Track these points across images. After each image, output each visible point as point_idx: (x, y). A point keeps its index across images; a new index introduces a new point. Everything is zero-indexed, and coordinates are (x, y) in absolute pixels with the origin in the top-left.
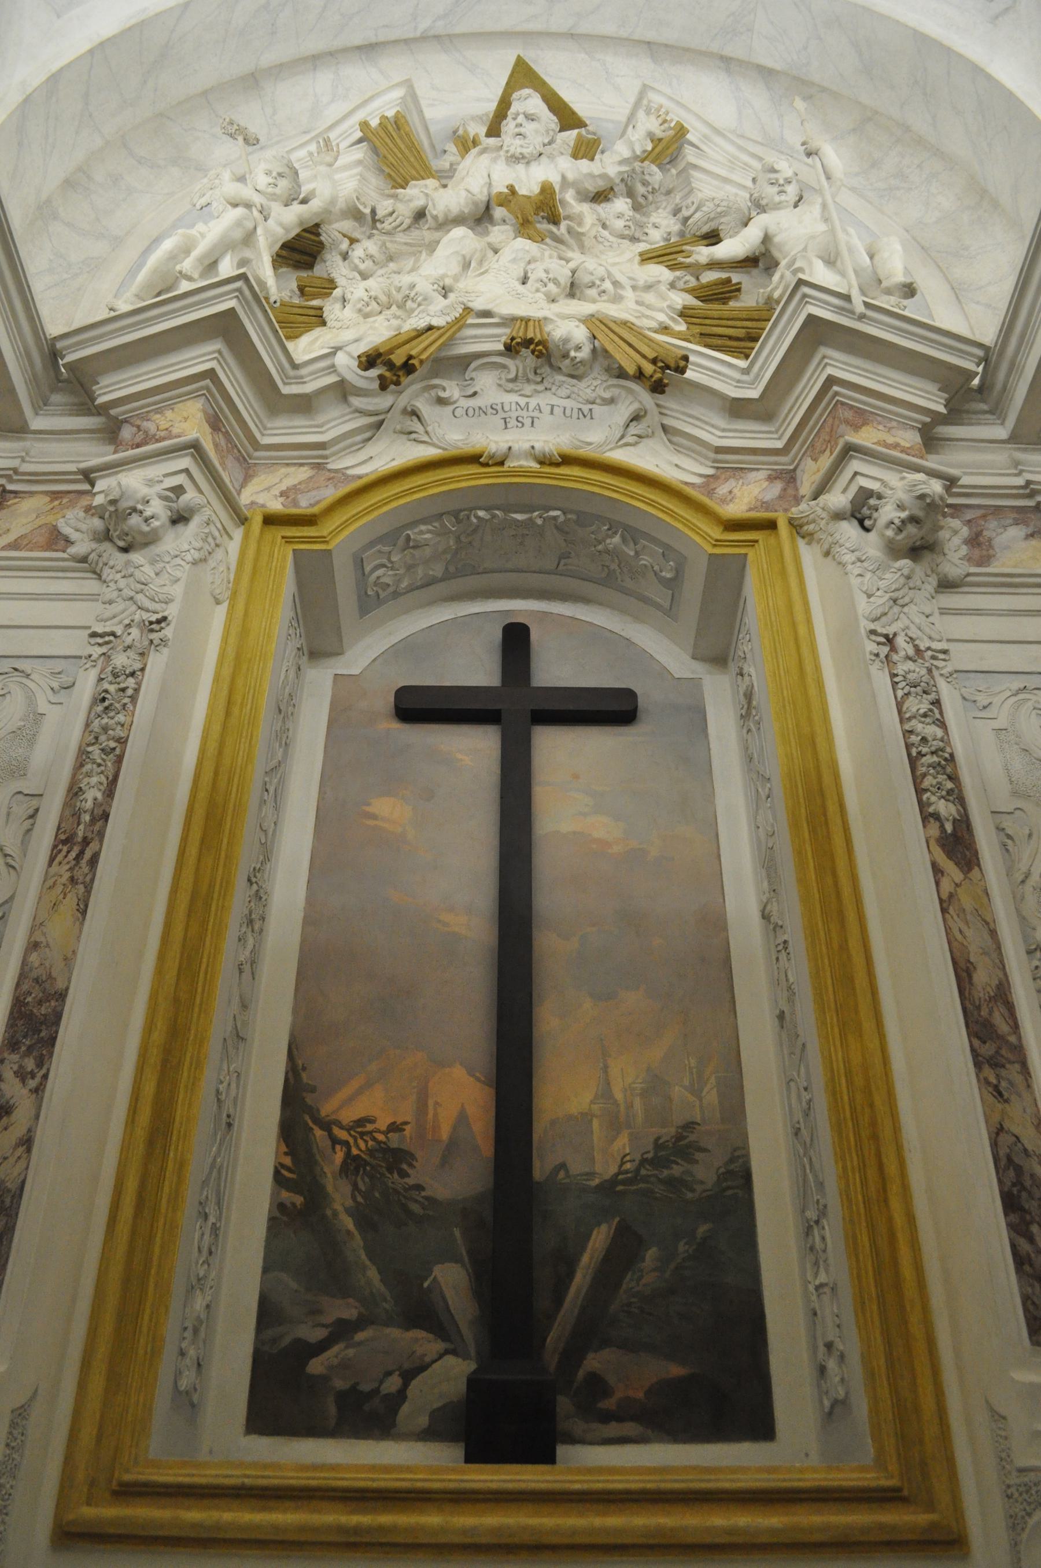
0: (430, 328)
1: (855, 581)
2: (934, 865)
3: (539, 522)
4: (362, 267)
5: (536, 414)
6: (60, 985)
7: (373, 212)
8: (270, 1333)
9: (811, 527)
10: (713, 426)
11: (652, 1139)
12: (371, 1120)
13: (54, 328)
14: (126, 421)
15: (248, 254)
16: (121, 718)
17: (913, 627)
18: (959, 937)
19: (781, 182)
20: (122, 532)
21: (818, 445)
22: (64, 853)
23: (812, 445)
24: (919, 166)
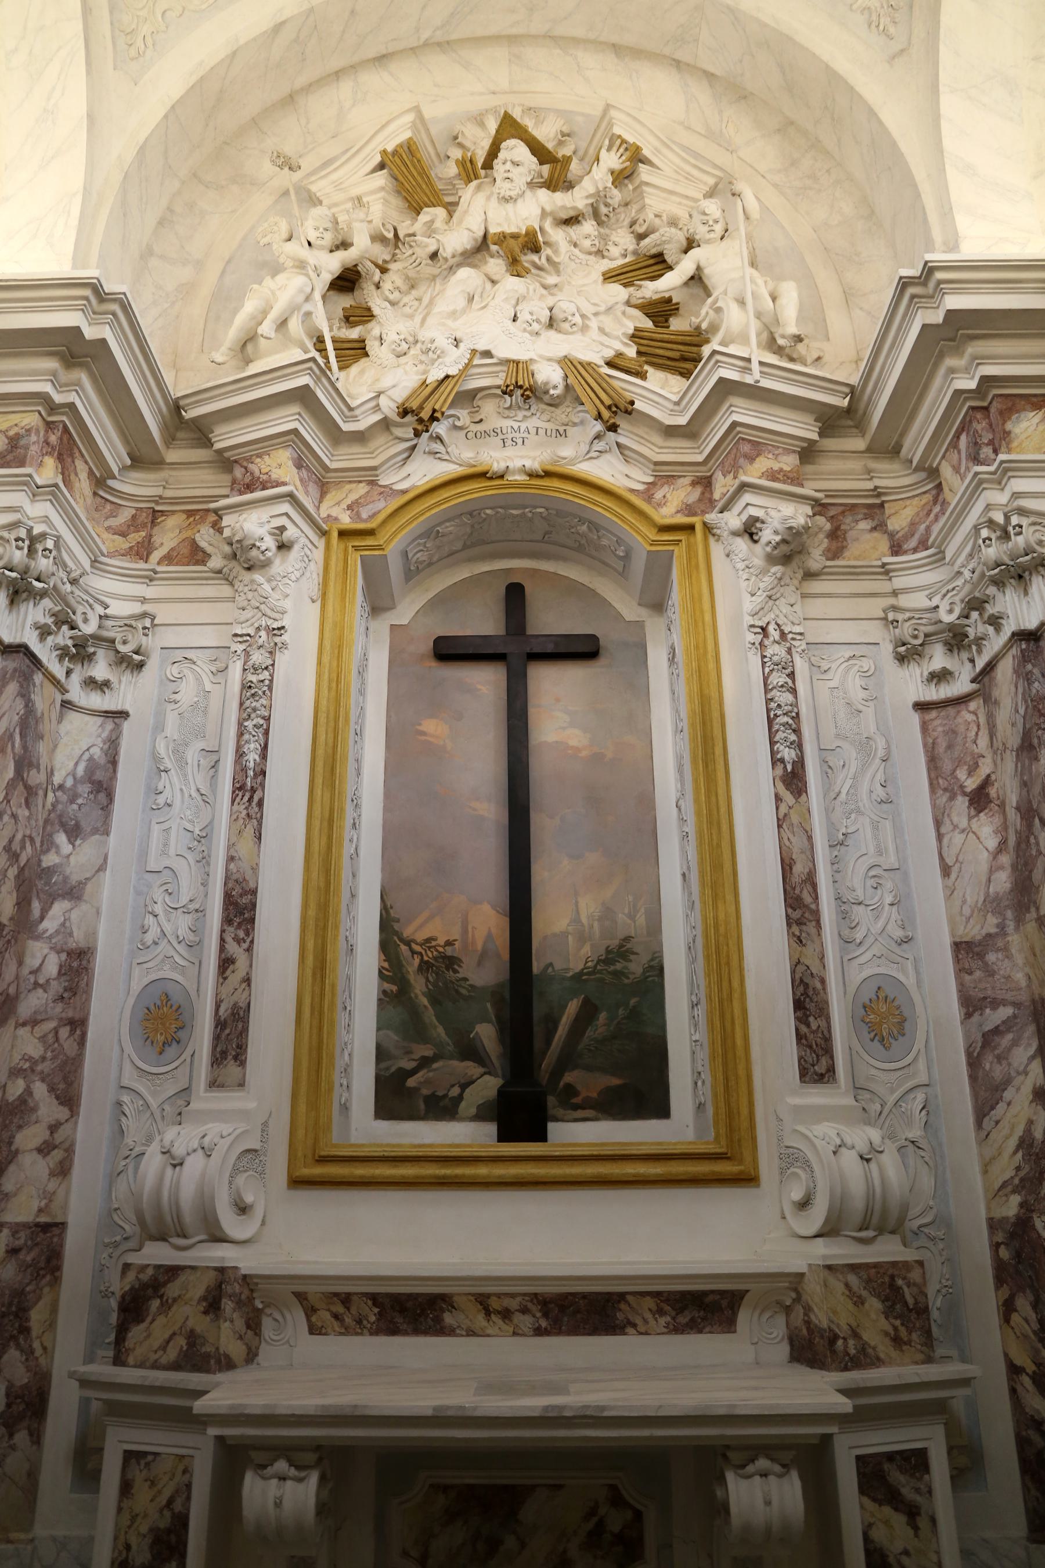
0: (447, 377)
1: (744, 584)
2: (777, 796)
3: (530, 515)
4: (391, 297)
5: (526, 435)
6: (252, 885)
7: (396, 235)
8: (383, 1065)
9: (718, 532)
11: (604, 947)
12: (435, 939)
13: (177, 390)
14: (236, 461)
15: (307, 307)
16: (263, 701)
17: (781, 616)
18: (787, 843)
19: (711, 223)
20: (244, 557)
21: (727, 464)
22: (240, 797)
23: (722, 462)
24: (828, 171)
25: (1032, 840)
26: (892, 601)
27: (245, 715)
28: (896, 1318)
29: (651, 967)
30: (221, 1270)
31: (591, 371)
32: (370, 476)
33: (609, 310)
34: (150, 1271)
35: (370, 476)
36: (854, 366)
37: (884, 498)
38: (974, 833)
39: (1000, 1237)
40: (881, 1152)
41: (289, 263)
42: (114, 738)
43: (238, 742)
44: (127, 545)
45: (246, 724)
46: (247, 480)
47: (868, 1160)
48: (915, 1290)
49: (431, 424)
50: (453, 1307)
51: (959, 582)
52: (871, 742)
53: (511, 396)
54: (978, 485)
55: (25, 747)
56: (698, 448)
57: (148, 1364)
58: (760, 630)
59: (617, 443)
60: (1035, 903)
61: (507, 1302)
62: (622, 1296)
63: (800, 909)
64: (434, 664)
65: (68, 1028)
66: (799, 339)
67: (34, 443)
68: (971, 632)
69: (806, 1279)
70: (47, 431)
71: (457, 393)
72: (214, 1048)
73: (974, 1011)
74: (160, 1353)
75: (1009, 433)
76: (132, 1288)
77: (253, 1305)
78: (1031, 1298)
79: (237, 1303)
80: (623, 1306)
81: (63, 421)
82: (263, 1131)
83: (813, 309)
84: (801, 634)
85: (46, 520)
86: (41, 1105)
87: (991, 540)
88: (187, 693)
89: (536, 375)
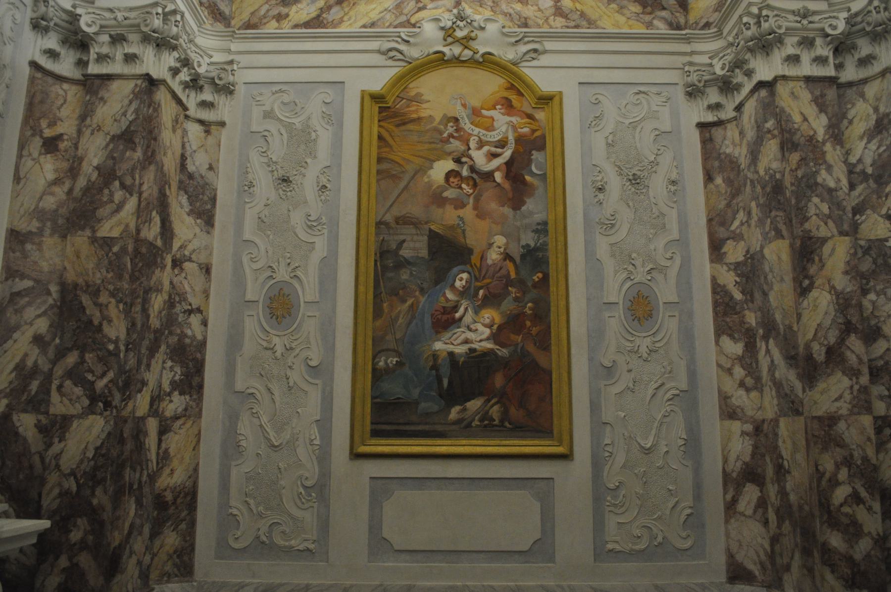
25: (106, 191)
51: (108, 15)
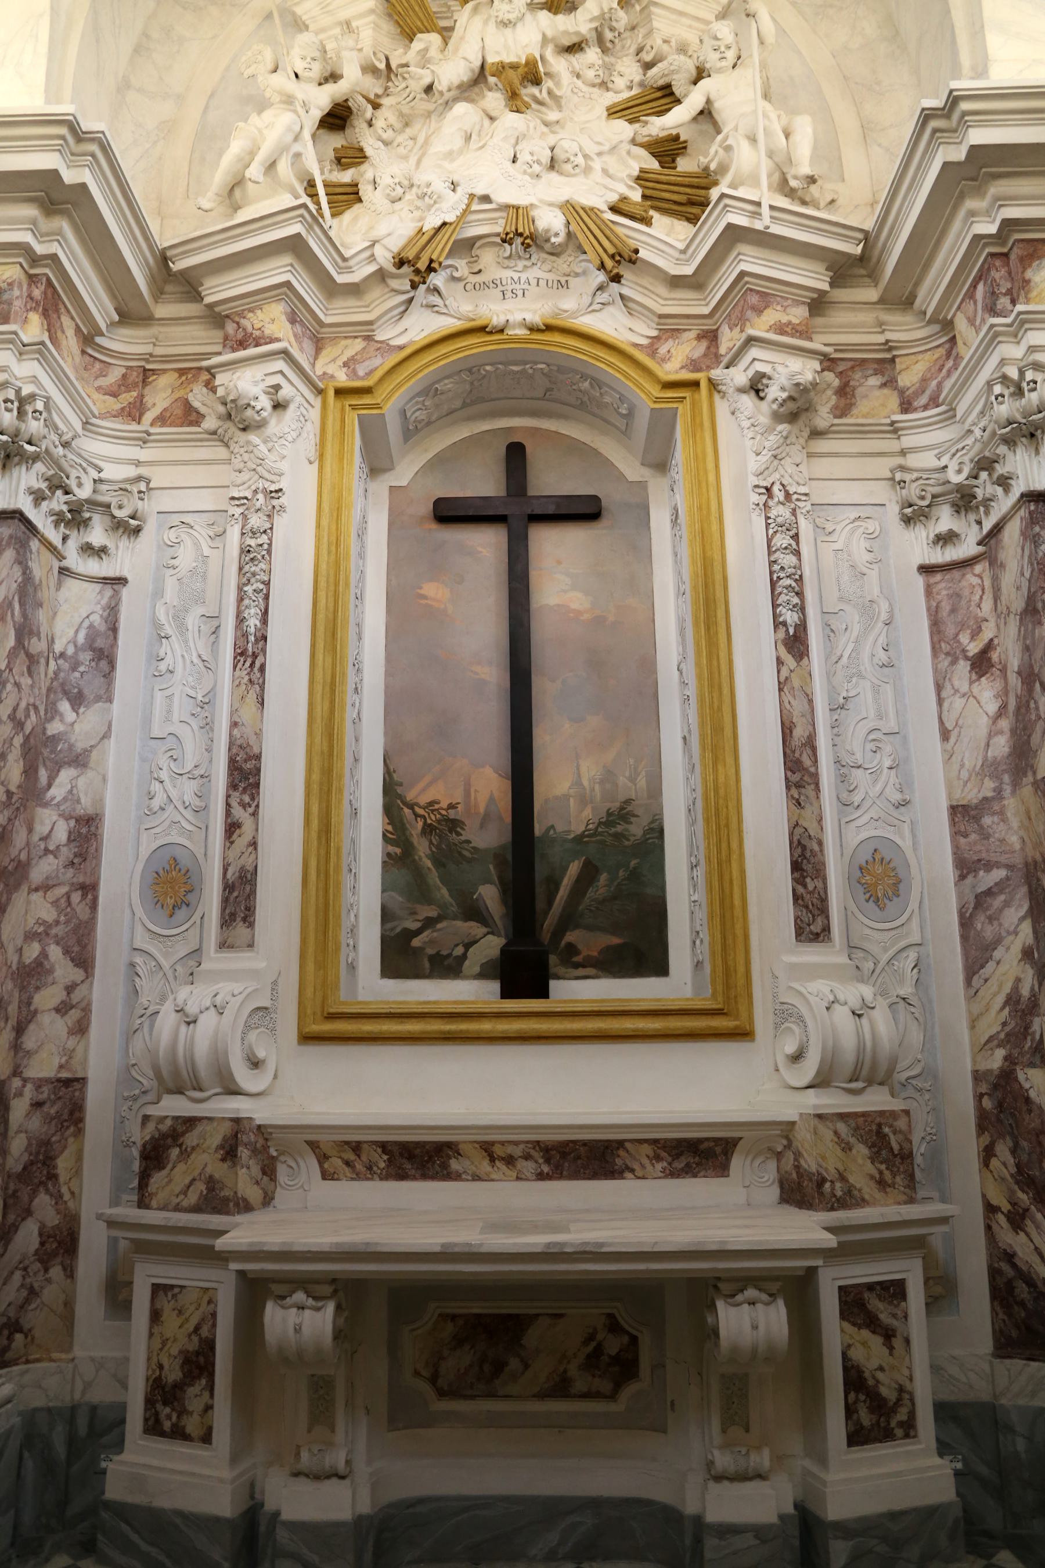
0: (444, 224)
2: (778, 659)
3: (530, 371)
4: (385, 136)
5: (526, 286)
6: (256, 750)
7: (388, 66)
8: (389, 926)
9: (723, 388)
10: (657, 295)
11: (605, 810)
13: (164, 241)
14: (227, 316)
15: (297, 148)
16: (262, 566)
17: (787, 476)
18: (788, 707)
20: (239, 418)
21: (733, 317)
23: (729, 315)
25: (1032, 705)
26: (899, 460)
27: (244, 580)
28: (881, 1163)
29: (652, 829)
30: (237, 1121)
31: (594, 217)
32: (365, 331)
33: (613, 149)
34: (169, 1122)
35: (365, 331)
36: (869, 209)
37: (895, 353)
38: (975, 697)
39: (984, 1088)
40: (873, 1008)
41: (276, 98)
42: (113, 605)
43: (238, 607)
44: (118, 406)
45: (246, 589)
46: (240, 335)
47: (860, 1016)
48: (901, 1137)
49: (428, 275)
50: (459, 1154)
51: (969, 441)
52: (875, 606)
53: (511, 244)
54: (994, 338)
55: (24, 615)
56: (705, 299)
57: (170, 1207)
58: (764, 491)
59: (620, 294)
60: (1032, 767)
61: (510, 1150)
62: (621, 1144)
63: (799, 772)
64: (434, 525)
65: (80, 893)
66: (812, 180)
67: (17, 298)
68: (979, 493)
69: (797, 1127)
70: (30, 285)
71: (455, 242)
72: (223, 910)
73: (968, 873)
74: (182, 1197)
75: (1028, 282)
76: (152, 1138)
77: (268, 1153)
78: (1010, 1143)
79: (253, 1151)
80: (621, 1152)
81: (46, 274)
82: (273, 989)
83: (828, 148)
84: (806, 495)
85: (34, 380)
86: (57, 966)
87: (1003, 396)
88: (186, 558)
89: (536, 222)
